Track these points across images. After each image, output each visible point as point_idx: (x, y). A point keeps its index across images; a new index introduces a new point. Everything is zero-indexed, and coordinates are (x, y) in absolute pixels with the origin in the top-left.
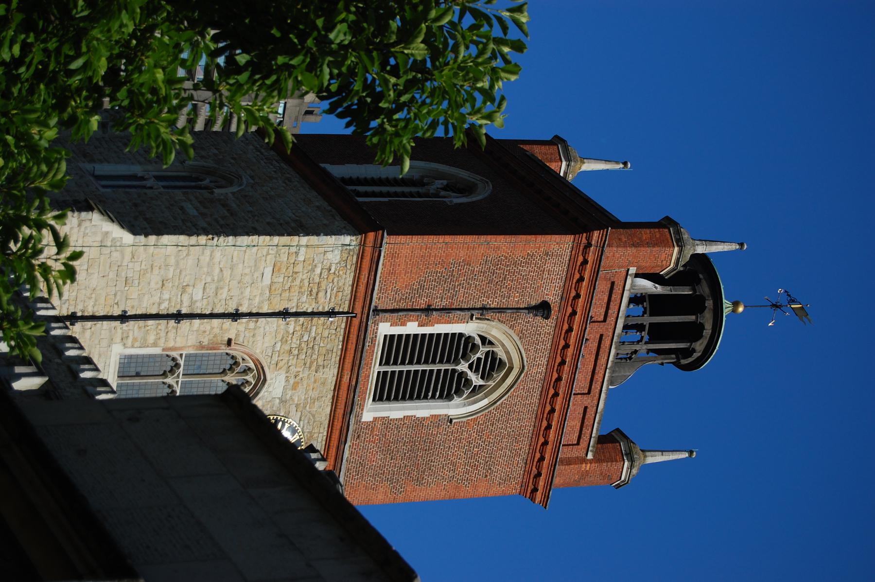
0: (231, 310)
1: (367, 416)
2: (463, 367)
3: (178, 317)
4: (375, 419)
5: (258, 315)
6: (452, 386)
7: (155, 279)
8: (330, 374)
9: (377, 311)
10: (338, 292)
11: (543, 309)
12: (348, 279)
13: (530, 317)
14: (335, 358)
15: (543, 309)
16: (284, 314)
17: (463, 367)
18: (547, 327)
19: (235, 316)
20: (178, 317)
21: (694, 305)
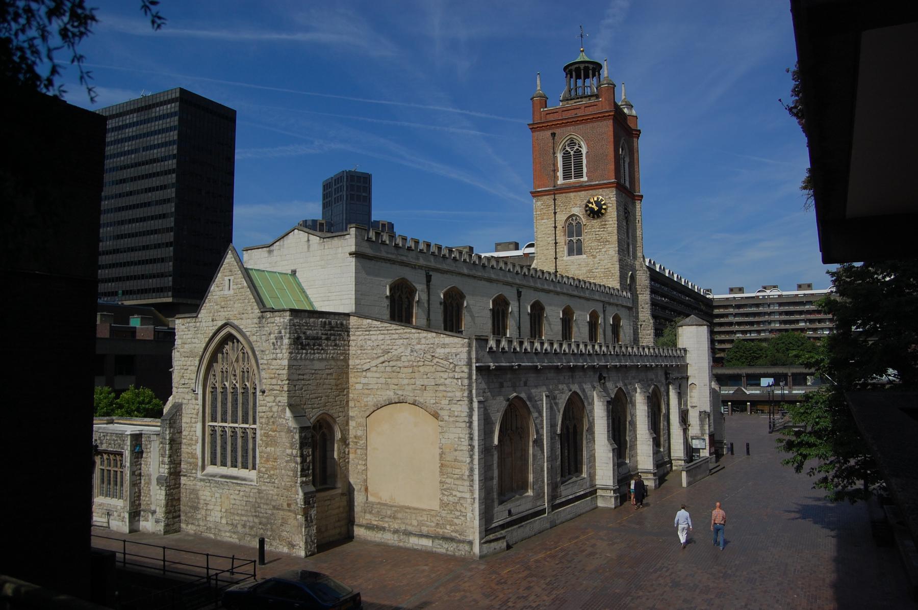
2: (572, 153)
3: (556, 243)
6: (578, 153)
7: (545, 252)
8: (572, 195)
10: (548, 200)
11: (553, 135)
15: (553, 135)
16: (555, 213)
17: (572, 153)
19: (555, 227)
21: (578, 71)
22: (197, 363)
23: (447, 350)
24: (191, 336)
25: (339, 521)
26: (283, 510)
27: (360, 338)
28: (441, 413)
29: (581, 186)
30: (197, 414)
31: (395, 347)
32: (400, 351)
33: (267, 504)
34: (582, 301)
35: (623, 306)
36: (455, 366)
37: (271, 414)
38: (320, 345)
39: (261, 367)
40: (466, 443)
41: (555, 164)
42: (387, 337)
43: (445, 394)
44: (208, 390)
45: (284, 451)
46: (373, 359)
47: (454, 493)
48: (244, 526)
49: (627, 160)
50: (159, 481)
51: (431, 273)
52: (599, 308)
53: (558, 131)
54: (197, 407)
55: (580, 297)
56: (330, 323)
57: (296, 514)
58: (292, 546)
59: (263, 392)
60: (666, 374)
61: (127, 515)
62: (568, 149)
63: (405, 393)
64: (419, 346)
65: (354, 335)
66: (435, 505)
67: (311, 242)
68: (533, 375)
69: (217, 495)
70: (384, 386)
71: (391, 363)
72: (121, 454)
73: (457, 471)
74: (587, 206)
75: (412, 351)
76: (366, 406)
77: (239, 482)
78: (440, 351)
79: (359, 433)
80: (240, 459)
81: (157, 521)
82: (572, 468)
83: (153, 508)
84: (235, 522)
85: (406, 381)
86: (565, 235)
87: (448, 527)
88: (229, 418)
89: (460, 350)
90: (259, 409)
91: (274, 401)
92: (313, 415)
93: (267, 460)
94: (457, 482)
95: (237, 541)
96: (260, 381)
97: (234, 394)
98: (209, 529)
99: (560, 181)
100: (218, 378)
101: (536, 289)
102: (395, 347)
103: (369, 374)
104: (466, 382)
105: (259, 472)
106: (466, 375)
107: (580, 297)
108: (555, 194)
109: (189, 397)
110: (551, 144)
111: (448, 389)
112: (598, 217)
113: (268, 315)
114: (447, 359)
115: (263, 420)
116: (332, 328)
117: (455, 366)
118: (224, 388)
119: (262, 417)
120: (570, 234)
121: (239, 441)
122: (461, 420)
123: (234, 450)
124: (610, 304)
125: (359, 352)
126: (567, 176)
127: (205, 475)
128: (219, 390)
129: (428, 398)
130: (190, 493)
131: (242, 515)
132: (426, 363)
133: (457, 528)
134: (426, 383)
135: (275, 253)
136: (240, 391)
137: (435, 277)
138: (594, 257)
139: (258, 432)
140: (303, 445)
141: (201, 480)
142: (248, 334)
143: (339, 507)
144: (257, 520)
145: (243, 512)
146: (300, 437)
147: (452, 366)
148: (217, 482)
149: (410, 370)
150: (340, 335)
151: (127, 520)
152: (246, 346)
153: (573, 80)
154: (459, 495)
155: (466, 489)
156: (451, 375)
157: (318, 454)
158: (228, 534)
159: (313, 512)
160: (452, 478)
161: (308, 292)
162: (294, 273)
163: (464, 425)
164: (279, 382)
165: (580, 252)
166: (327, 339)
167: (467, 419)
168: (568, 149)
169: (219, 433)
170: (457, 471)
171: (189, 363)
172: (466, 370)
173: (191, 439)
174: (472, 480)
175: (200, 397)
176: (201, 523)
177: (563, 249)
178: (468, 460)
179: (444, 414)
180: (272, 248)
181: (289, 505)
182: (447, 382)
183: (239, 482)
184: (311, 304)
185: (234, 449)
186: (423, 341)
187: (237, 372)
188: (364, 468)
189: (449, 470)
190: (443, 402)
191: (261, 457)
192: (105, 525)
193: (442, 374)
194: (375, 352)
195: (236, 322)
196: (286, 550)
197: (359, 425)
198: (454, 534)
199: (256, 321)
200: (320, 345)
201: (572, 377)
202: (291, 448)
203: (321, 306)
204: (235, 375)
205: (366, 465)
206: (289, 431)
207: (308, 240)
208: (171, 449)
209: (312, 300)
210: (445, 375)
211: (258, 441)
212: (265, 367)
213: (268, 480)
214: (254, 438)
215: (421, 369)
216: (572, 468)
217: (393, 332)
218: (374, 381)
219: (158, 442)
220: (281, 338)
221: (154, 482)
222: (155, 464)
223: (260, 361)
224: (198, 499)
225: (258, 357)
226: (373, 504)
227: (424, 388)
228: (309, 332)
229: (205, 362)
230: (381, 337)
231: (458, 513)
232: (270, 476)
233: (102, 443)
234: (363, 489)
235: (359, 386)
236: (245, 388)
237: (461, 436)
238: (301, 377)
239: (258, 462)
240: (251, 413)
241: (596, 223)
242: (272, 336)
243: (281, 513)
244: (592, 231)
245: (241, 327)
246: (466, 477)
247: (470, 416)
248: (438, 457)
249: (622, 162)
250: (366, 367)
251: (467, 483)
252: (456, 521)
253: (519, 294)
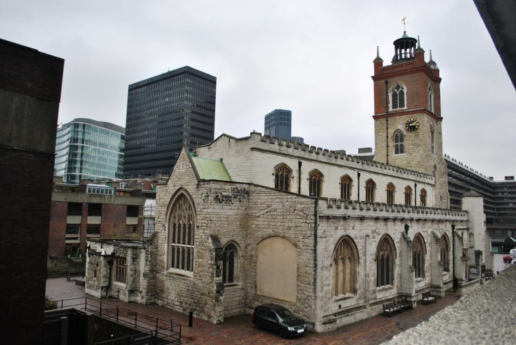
0: (386, 138)
2: (398, 93)
3: (388, 146)
4: (407, 106)
5: (387, 133)
6: (402, 93)
7: (381, 151)
8: (398, 117)
9: (387, 113)
11: (387, 82)
12: (381, 119)
13: (388, 84)
14: (395, 118)
15: (387, 82)
16: (387, 128)
17: (398, 93)
18: (389, 80)
19: (387, 137)
20: (388, 146)
22: (166, 210)
23: (303, 206)
24: (163, 195)
25: (239, 304)
26: (206, 296)
27: (255, 198)
28: (299, 244)
29: (403, 112)
30: (165, 239)
31: (274, 203)
32: (276, 206)
33: (198, 291)
34: (401, 180)
35: (428, 184)
36: (307, 215)
37: (201, 240)
38: (231, 201)
39: (197, 213)
40: (312, 262)
42: (270, 197)
43: (301, 232)
44: (171, 225)
45: (207, 262)
46: (261, 210)
47: (305, 292)
48: (186, 303)
49: (433, 96)
50: (145, 275)
51: (301, 161)
52: (412, 185)
53: (389, 80)
54: (165, 234)
55: (399, 178)
56: (237, 188)
57: (212, 299)
58: (210, 317)
59: (198, 227)
60: (453, 227)
61: (127, 293)
62: (396, 91)
63: (278, 231)
64: (287, 203)
65: (252, 196)
66: (294, 300)
67: (230, 142)
68: (359, 223)
69: (173, 285)
70: (267, 226)
71: (272, 213)
72: (125, 259)
73: (307, 279)
74: (406, 124)
75: (283, 206)
76: (257, 238)
77: (184, 278)
78: (299, 206)
79: (253, 253)
80: (186, 265)
81: (143, 297)
82: (385, 282)
83: (141, 289)
84: (182, 301)
85: (279, 224)
86: (393, 141)
87: (301, 313)
88: (181, 242)
89: (310, 206)
90: (196, 237)
91: (203, 233)
92: (224, 241)
93: (199, 266)
94: (306, 286)
95: (182, 311)
96: (196, 221)
97: (184, 228)
98: (168, 304)
99: (391, 109)
100: (177, 219)
101: (370, 172)
102: (274, 203)
103: (259, 219)
104: (313, 225)
105: (195, 273)
106: (313, 221)
107: (399, 178)
108: (387, 117)
110: (385, 88)
111: (303, 229)
112: (414, 130)
113: (202, 183)
114: (302, 211)
116: (238, 192)
117: (307, 215)
118: (180, 224)
119: (197, 242)
120: (397, 141)
121: (186, 255)
122: (310, 248)
123: (183, 260)
124: (419, 182)
125: (254, 206)
126: (394, 106)
127: (168, 273)
128: (177, 225)
129: (291, 234)
130: (160, 283)
131: (185, 297)
132: (291, 213)
133: (306, 314)
134: (290, 225)
135: (212, 149)
136: (187, 226)
137: (304, 163)
138: (411, 154)
139: (195, 250)
140: (217, 258)
141: (166, 276)
142: (191, 194)
143: (240, 296)
144: (192, 300)
145: (186, 295)
146: (216, 254)
147: (305, 215)
148: (174, 278)
149: (282, 217)
150: (244, 196)
151: (127, 295)
152: (190, 200)
153: (398, 50)
154: (307, 294)
155: (311, 290)
156: (305, 221)
157: (227, 264)
158: (178, 307)
159: (222, 298)
160: (304, 283)
161: (229, 171)
162: (221, 160)
163: (311, 251)
164: (206, 222)
165: (402, 152)
166: (235, 198)
167: (313, 248)
169: (176, 249)
170: (307, 279)
171: (162, 210)
172: (313, 218)
173: (162, 253)
174: (315, 286)
175: (167, 229)
176: (165, 300)
177: (392, 150)
178: (313, 273)
179: (300, 244)
180: (210, 146)
181: (209, 293)
182: (303, 225)
183: (184, 278)
184: (230, 178)
185: (183, 259)
186: (289, 200)
187: (186, 215)
188: (255, 274)
189: (303, 278)
190: (300, 237)
192: (117, 297)
193: (300, 220)
194: (263, 206)
195: (186, 187)
196: (206, 319)
197: (253, 248)
198: (304, 318)
199: (196, 186)
200: (231, 201)
201: (386, 225)
202: (211, 260)
203: (234, 179)
204: (185, 217)
205: (256, 272)
206: (210, 250)
207: (229, 141)
208: (151, 257)
209: (231, 175)
210: (301, 221)
211: (195, 255)
212: (199, 213)
213: (199, 278)
214: (193, 254)
215: (288, 217)
216: (385, 282)
217: (273, 194)
218: (262, 223)
219: (144, 253)
220: (208, 196)
221: (142, 275)
222: (143, 267)
223: (197, 210)
224: (164, 286)
225: (196, 207)
226: (259, 295)
227: (289, 228)
228: (224, 194)
229: (170, 209)
230: (266, 197)
231: (307, 305)
232: (200, 276)
233: (117, 252)
234: (254, 286)
235: (254, 226)
236: (190, 225)
237: (310, 258)
238: (219, 219)
239: (194, 267)
240: (192, 239)
241: (412, 134)
242: (203, 195)
243: (205, 297)
244: (409, 140)
245: (188, 190)
246: (312, 283)
247: (315, 246)
248: (296, 270)
249: (429, 97)
250: (258, 214)
251: (312, 287)
252: (305, 309)
253: (359, 175)
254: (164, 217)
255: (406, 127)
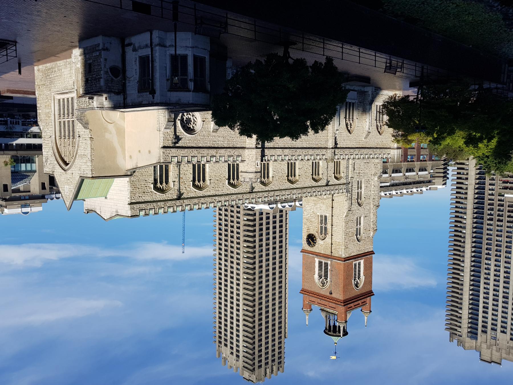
1: (316, 259)
2: (323, 278)
8: (322, 252)
10: (335, 254)
11: (331, 294)
14: (324, 253)
17: (323, 278)
20: (332, 225)
22: (79, 151)
24: (83, 166)
41: (331, 274)
48: (55, 71)
95: (58, 62)
109: (83, 133)
115: (50, 124)
120: (326, 228)
144: (50, 76)
158: (61, 64)
165: (321, 216)
168: (325, 282)
180: (116, 214)
191: (51, 107)
239: (53, 104)
241: (312, 232)
254: (80, 144)
255: (316, 240)
